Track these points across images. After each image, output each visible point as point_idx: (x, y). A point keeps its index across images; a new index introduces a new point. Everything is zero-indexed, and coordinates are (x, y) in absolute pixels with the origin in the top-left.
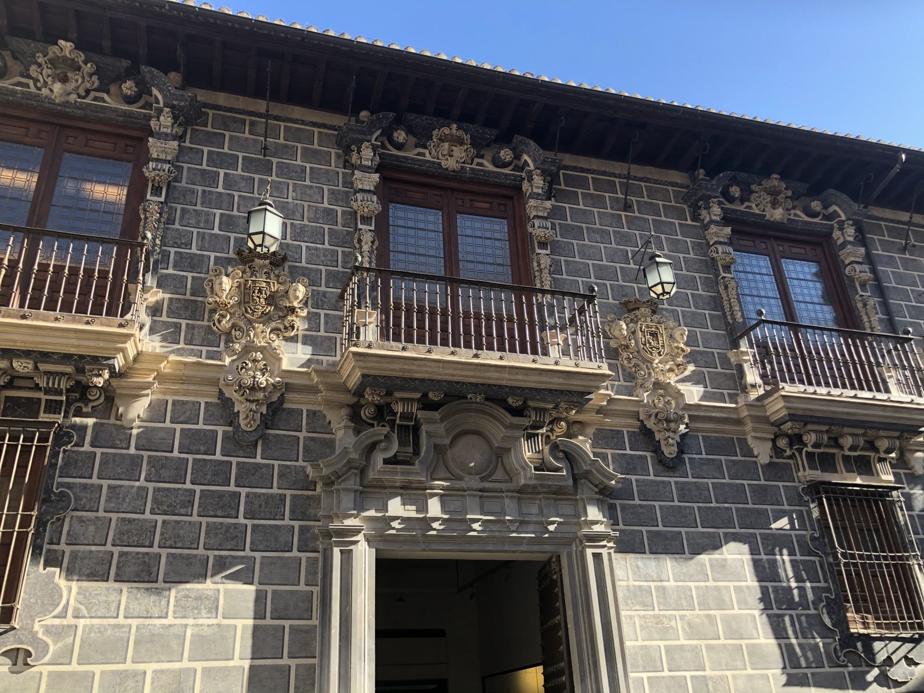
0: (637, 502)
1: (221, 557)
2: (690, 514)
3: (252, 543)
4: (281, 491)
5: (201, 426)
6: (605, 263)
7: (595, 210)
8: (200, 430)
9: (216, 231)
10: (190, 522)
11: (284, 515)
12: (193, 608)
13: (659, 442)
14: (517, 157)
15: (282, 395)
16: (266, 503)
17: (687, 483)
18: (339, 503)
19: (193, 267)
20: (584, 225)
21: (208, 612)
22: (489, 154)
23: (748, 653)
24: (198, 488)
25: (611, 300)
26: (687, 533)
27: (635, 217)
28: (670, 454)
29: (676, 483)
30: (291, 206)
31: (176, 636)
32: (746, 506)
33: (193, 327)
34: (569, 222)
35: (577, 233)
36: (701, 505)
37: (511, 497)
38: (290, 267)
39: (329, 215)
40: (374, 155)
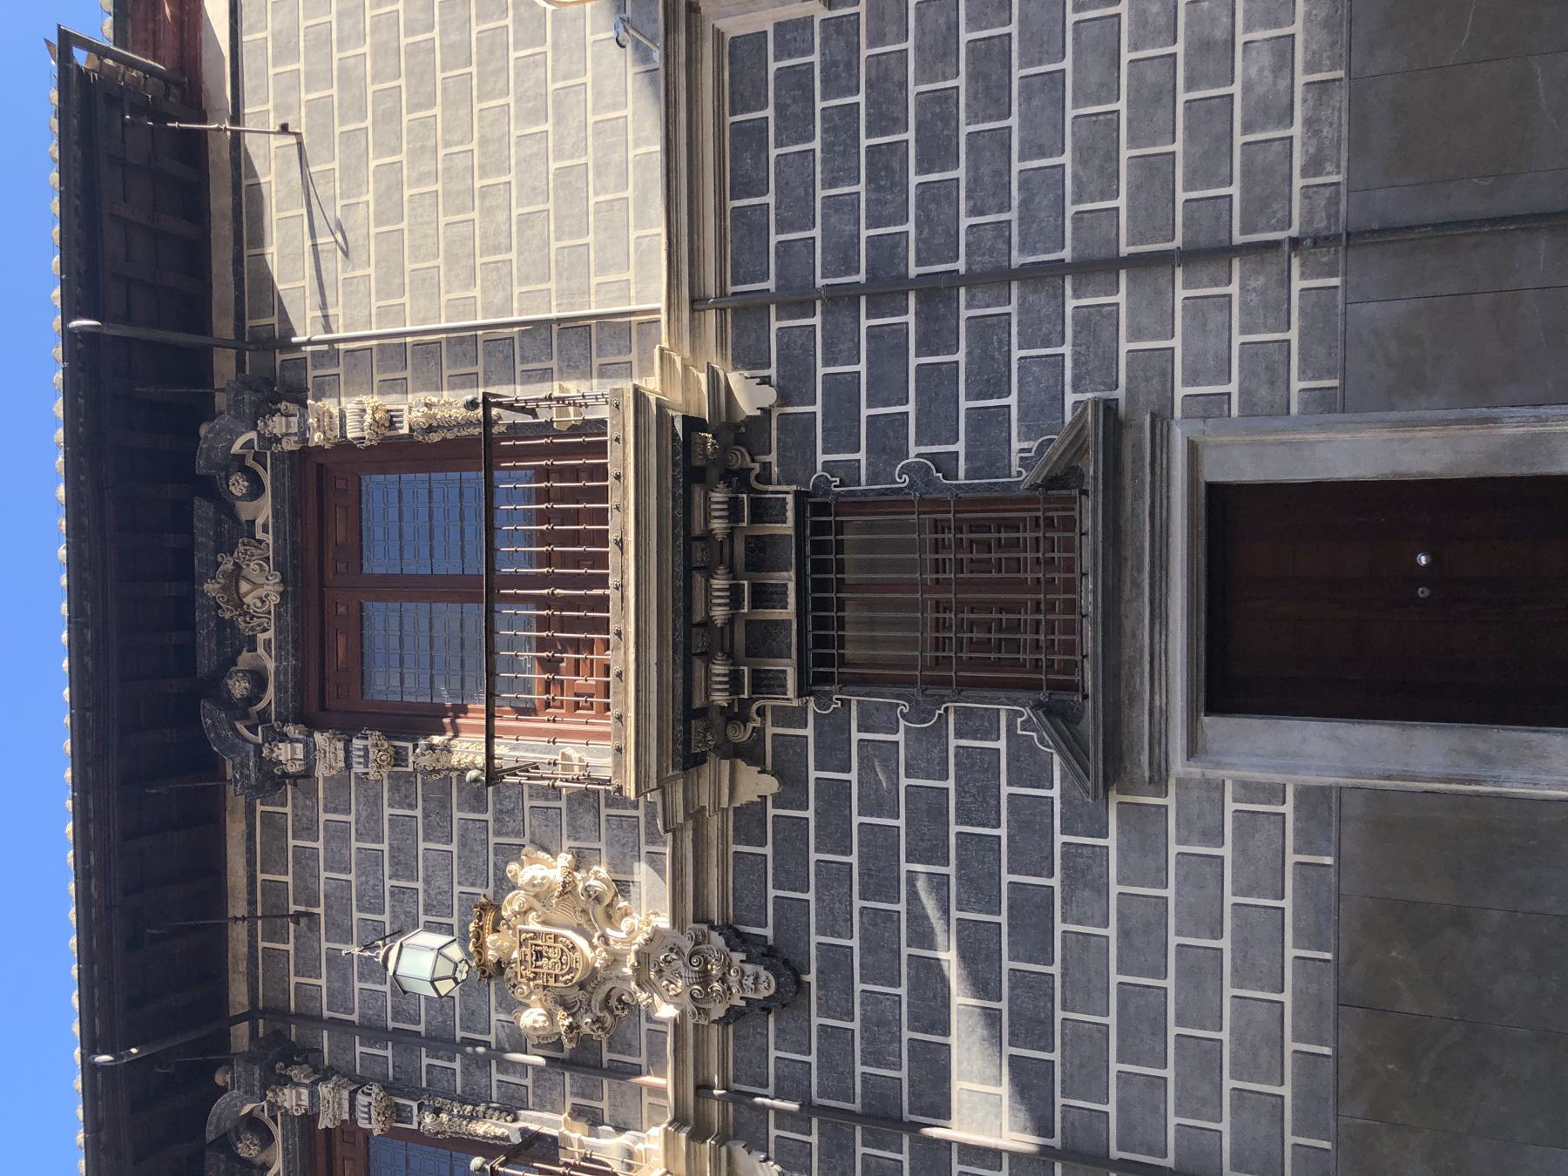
14: (238, 464)
15: (712, 927)
22: (245, 510)
40: (284, 738)
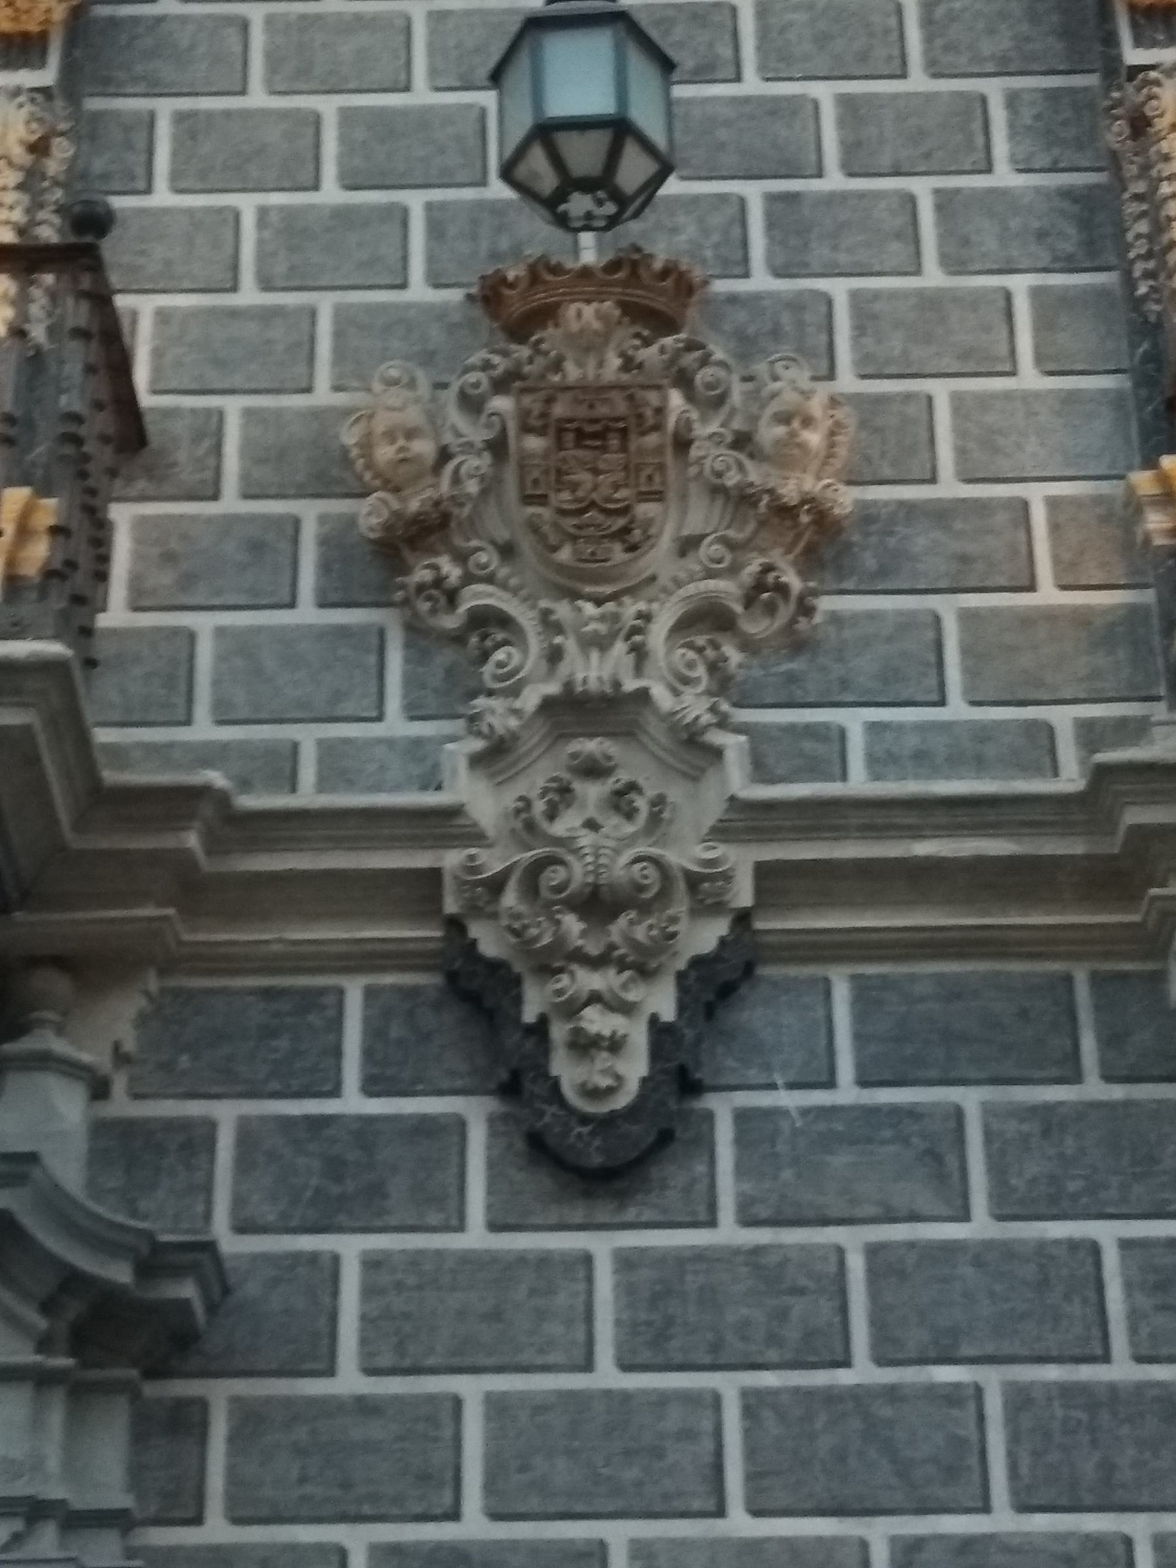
0: (349, 1380)
6: (422, 95)
13: (540, 1029)
17: (700, 1256)
25: (419, 291)
28: (594, 1093)
32: (1086, 1373)
36: (769, 1379)
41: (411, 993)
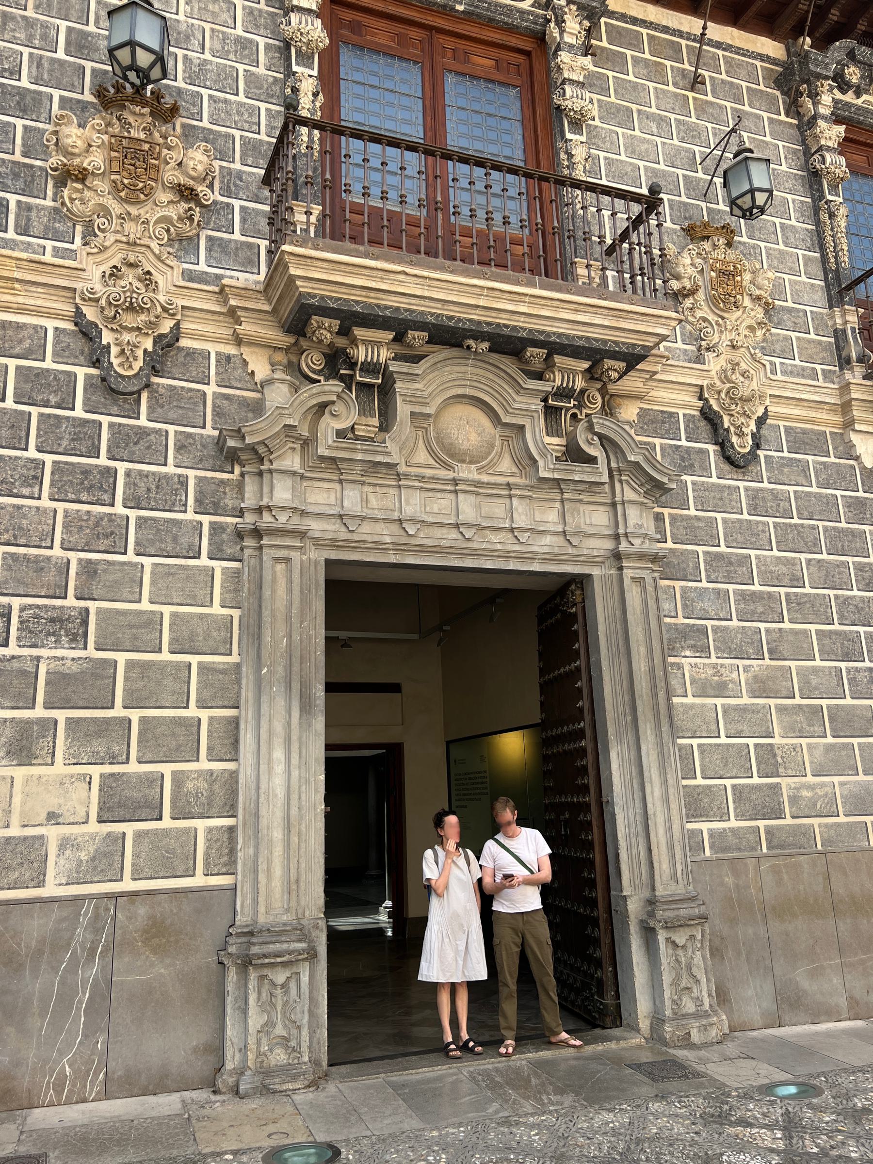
0: (692, 512)
1: (89, 561)
2: (763, 531)
3: (137, 543)
4: (180, 471)
5: (48, 364)
6: (662, 167)
7: (651, 85)
8: (48, 370)
9: (61, 54)
10: (38, 508)
11: (185, 505)
12: (49, 634)
15: (177, 325)
16: (158, 487)
17: (761, 489)
18: (271, 492)
19: (24, 111)
20: (634, 107)
21: (72, 641)
23: (830, 717)
24: (49, 459)
26: (758, 557)
27: (707, 102)
29: (747, 489)
30: (183, 27)
31: (23, 673)
32: (837, 524)
33: (29, 208)
34: (613, 99)
35: (624, 117)
37: (521, 497)
38: (184, 126)
39: (245, 48)
41: (694, 416)
